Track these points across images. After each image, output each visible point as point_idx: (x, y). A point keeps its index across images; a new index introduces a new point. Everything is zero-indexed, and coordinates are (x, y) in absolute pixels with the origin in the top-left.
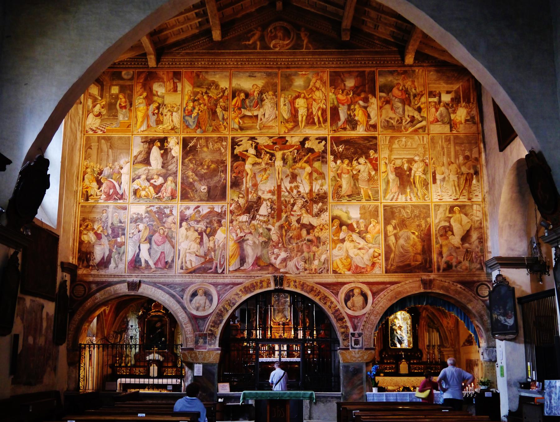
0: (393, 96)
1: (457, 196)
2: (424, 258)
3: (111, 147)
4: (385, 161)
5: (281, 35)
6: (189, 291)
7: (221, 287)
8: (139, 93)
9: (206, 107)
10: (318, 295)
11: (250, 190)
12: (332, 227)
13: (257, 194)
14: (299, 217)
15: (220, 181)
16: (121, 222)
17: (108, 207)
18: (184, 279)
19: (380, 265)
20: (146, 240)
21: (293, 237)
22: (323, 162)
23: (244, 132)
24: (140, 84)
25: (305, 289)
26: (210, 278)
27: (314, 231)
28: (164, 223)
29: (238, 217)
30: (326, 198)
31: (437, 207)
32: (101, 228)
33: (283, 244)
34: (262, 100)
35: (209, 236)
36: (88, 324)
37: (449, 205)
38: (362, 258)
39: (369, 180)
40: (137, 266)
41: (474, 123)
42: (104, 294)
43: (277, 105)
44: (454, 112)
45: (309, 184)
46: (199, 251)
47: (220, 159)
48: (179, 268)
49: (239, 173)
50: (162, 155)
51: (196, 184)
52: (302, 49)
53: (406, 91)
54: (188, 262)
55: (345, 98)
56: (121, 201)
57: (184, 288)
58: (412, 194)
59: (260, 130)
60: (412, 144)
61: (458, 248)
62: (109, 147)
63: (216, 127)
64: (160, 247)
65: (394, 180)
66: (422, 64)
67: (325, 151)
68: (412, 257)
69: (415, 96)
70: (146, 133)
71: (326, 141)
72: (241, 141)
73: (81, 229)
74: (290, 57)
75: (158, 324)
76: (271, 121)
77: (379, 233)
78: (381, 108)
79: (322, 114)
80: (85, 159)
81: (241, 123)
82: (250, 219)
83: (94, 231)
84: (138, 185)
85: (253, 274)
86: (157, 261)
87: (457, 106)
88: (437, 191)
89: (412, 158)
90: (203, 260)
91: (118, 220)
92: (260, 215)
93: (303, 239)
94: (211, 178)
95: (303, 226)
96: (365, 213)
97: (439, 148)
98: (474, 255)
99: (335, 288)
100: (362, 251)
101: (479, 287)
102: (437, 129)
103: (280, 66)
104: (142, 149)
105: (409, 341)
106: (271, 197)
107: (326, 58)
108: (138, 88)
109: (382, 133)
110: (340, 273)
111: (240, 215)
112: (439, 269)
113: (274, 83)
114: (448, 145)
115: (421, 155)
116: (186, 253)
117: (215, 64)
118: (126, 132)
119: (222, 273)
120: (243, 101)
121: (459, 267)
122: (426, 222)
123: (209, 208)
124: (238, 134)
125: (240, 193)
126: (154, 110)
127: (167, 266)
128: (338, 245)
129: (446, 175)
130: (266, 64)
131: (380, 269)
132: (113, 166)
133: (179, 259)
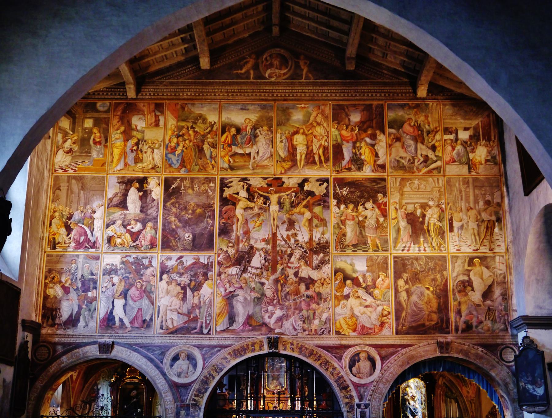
0: (404, 133)
1: (478, 247)
2: (440, 317)
3: (83, 188)
4: (395, 205)
5: (278, 63)
6: (170, 354)
7: (206, 350)
8: (116, 127)
9: (191, 144)
10: (319, 360)
11: (241, 238)
12: (335, 281)
13: (249, 243)
14: (297, 270)
15: (206, 227)
16: (92, 274)
17: (78, 256)
18: (164, 341)
19: (390, 325)
20: (120, 295)
21: (290, 292)
22: (324, 207)
23: (234, 173)
24: (117, 117)
25: (303, 352)
26: (194, 339)
27: (314, 286)
28: (142, 275)
29: (227, 269)
30: (328, 248)
31: (454, 259)
32: (70, 281)
33: (279, 301)
34: (256, 136)
35: (193, 290)
36: (51, 392)
37: (468, 256)
38: (370, 317)
39: (377, 228)
40: (110, 325)
41: (496, 164)
42: (72, 357)
43: (272, 142)
44: (473, 151)
45: (309, 232)
46: (181, 308)
47: (207, 202)
49: (229, 218)
50: (141, 198)
51: (179, 231)
52: (302, 79)
53: (419, 127)
54: (168, 321)
55: (349, 134)
56: (93, 250)
57: (164, 349)
58: (426, 244)
59: (253, 170)
60: (425, 187)
61: (479, 306)
62: (80, 188)
63: (203, 166)
64: (137, 303)
65: (405, 228)
66: (436, 97)
67: (327, 195)
68: (426, 316)
69: (429, 133)
70: (123, 172)
71: (328, 183)
72: (231, 182)
73: (47, 281)
74: (288, 88)
75: (134, 393)
76: (266, 160)
77: (388, 288)
78: (390, 146)
79: (324, 152)
80: (53, 201)
81: (232, 162)
82: (241, 272)
83: (61, 284)
84: (113, 232)
85: (244, 335)
86: (133, 320)
87: (476, 144)
88: (454, 240)
89: (426, 203)
90: (186, 318)
91: (89, 272)
92: (253, 267)
93: (302, 294)
94: (196, 224)
95: (302, 280)
96: (373, 265)
97: (456, 192)
98: (497, 314)
99: (338, 351)
100: (369, 309)
101: (503, 351)
102: (453, 170)
103: (277, 98)
104: (118, 191)
105: (423, 413)
106: (265, 246)
107: (329, 90)
108: (115, 122)
109: (392, 174)
110: (344, 335)
111: (229, 267)
112: (457, 330)
113: (269, 117)
114: (466, 188)
115: (436, 199)
116: (166, 310)
117: (203, 95)
118: (101, 171)
119: (208, 333)
120: (234, 136)
121: (480, 327)
122: (443, 275)
123: (194, 259)
124: (228, 175)
125: (230, 242)
126: (133, 147)
127: (145, 326)
128: (342, 302)
129: (464, 222)
130: (260, 95)
131: (389, 329)
132: (85, 210)
133: (158, 317)
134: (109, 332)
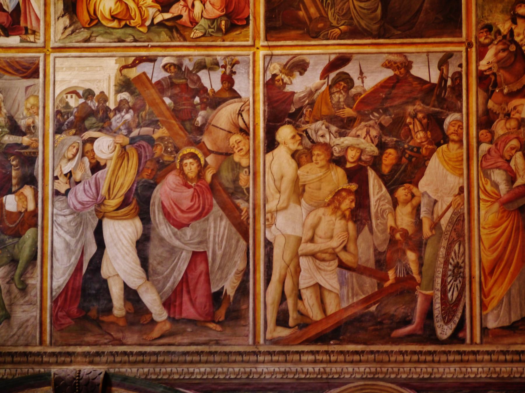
20: (125, 204)
28: (200, 130)
29: (515, 102)
40: (93, 313)
46: (351, 247)
48: (271, 318)
56: (14, 40)
64: (188, 231)
86: (177, 292)
116: (296, 256)
123: (388, 65)
133: (268, 281)
134: (90, 338)
